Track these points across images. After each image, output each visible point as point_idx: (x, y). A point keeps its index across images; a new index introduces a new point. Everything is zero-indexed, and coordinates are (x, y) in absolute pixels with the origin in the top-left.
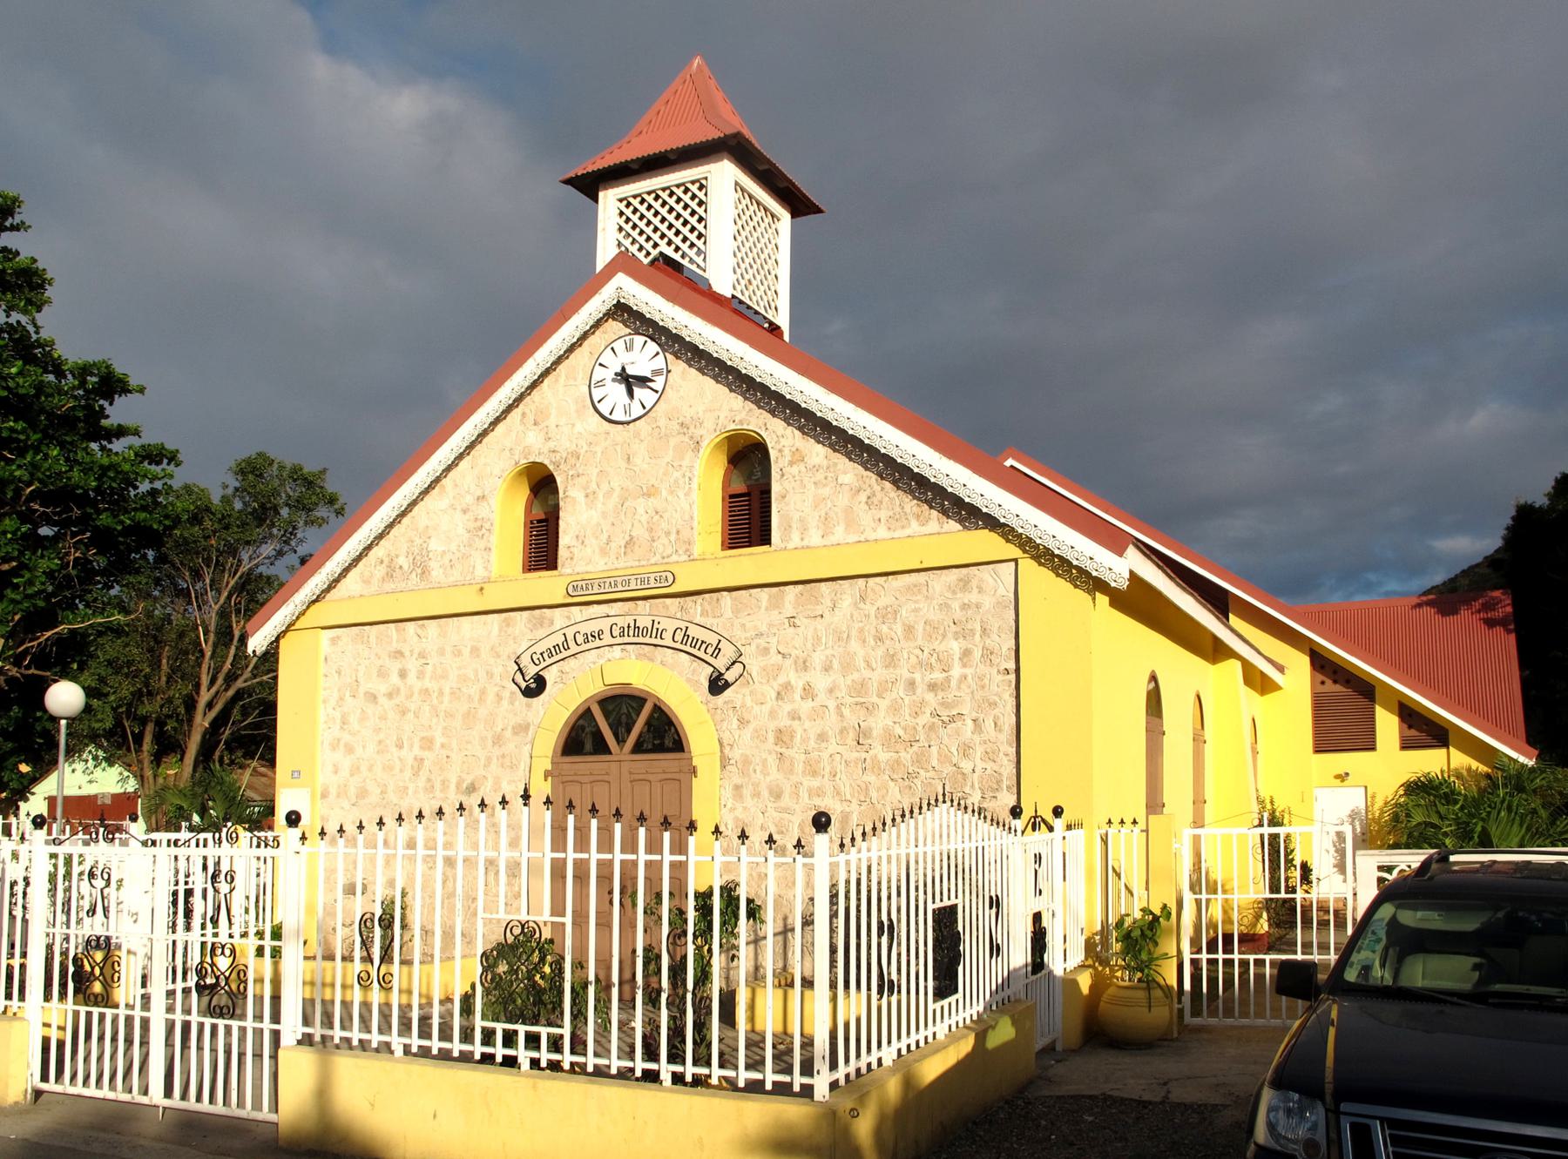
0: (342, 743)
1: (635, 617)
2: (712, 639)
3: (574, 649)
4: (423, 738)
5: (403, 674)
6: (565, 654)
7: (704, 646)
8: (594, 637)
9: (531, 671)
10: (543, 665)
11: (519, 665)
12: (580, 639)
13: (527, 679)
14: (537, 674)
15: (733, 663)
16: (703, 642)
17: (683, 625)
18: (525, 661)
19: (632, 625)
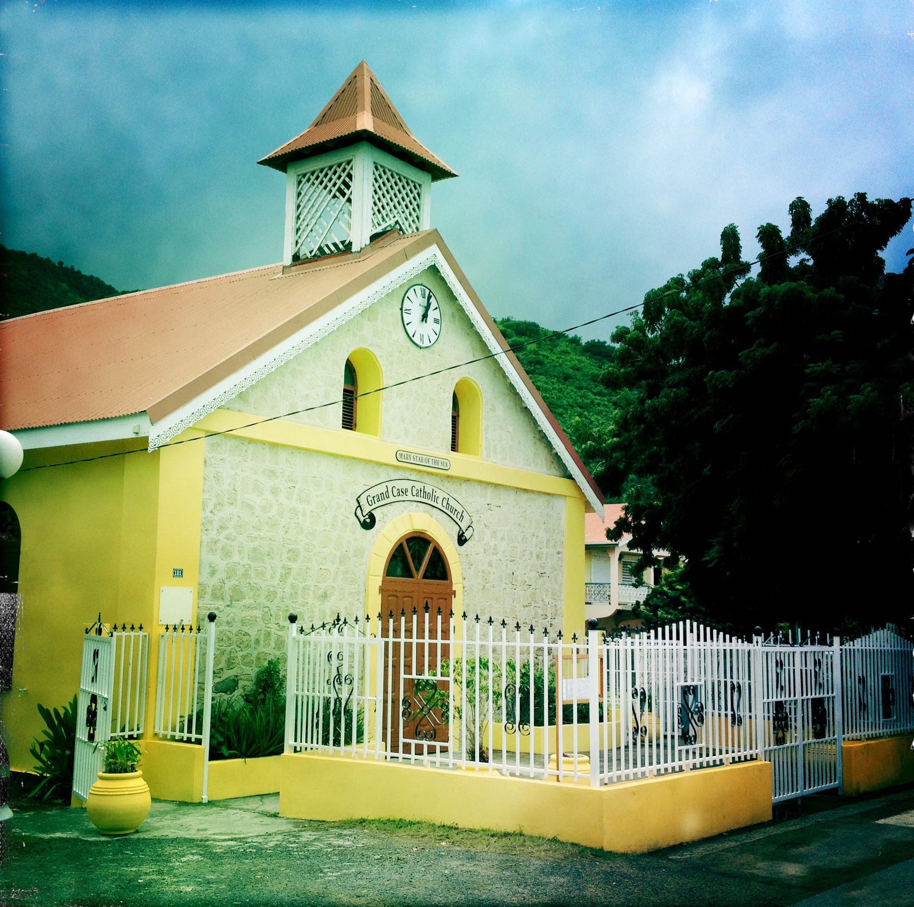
0: (220, 545)
1: (425, 485)
2: (460, 509)
3: (392, 499)
4: (290, 550)
5: (275, 491)
6: (387, 501)
7: (456, 512)
8: (403, 492)
9: (367, 509)
10: (374, 506)
11: (359, 503)
12: (395, 493)
13: (364, 515)
14: (370, 512)
15: (469, 527)
16: (456, 510)
17: (447, 497)
18: (363, 501)
19: (422, 489)
